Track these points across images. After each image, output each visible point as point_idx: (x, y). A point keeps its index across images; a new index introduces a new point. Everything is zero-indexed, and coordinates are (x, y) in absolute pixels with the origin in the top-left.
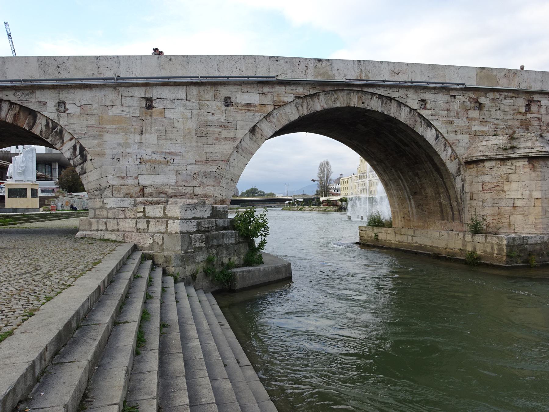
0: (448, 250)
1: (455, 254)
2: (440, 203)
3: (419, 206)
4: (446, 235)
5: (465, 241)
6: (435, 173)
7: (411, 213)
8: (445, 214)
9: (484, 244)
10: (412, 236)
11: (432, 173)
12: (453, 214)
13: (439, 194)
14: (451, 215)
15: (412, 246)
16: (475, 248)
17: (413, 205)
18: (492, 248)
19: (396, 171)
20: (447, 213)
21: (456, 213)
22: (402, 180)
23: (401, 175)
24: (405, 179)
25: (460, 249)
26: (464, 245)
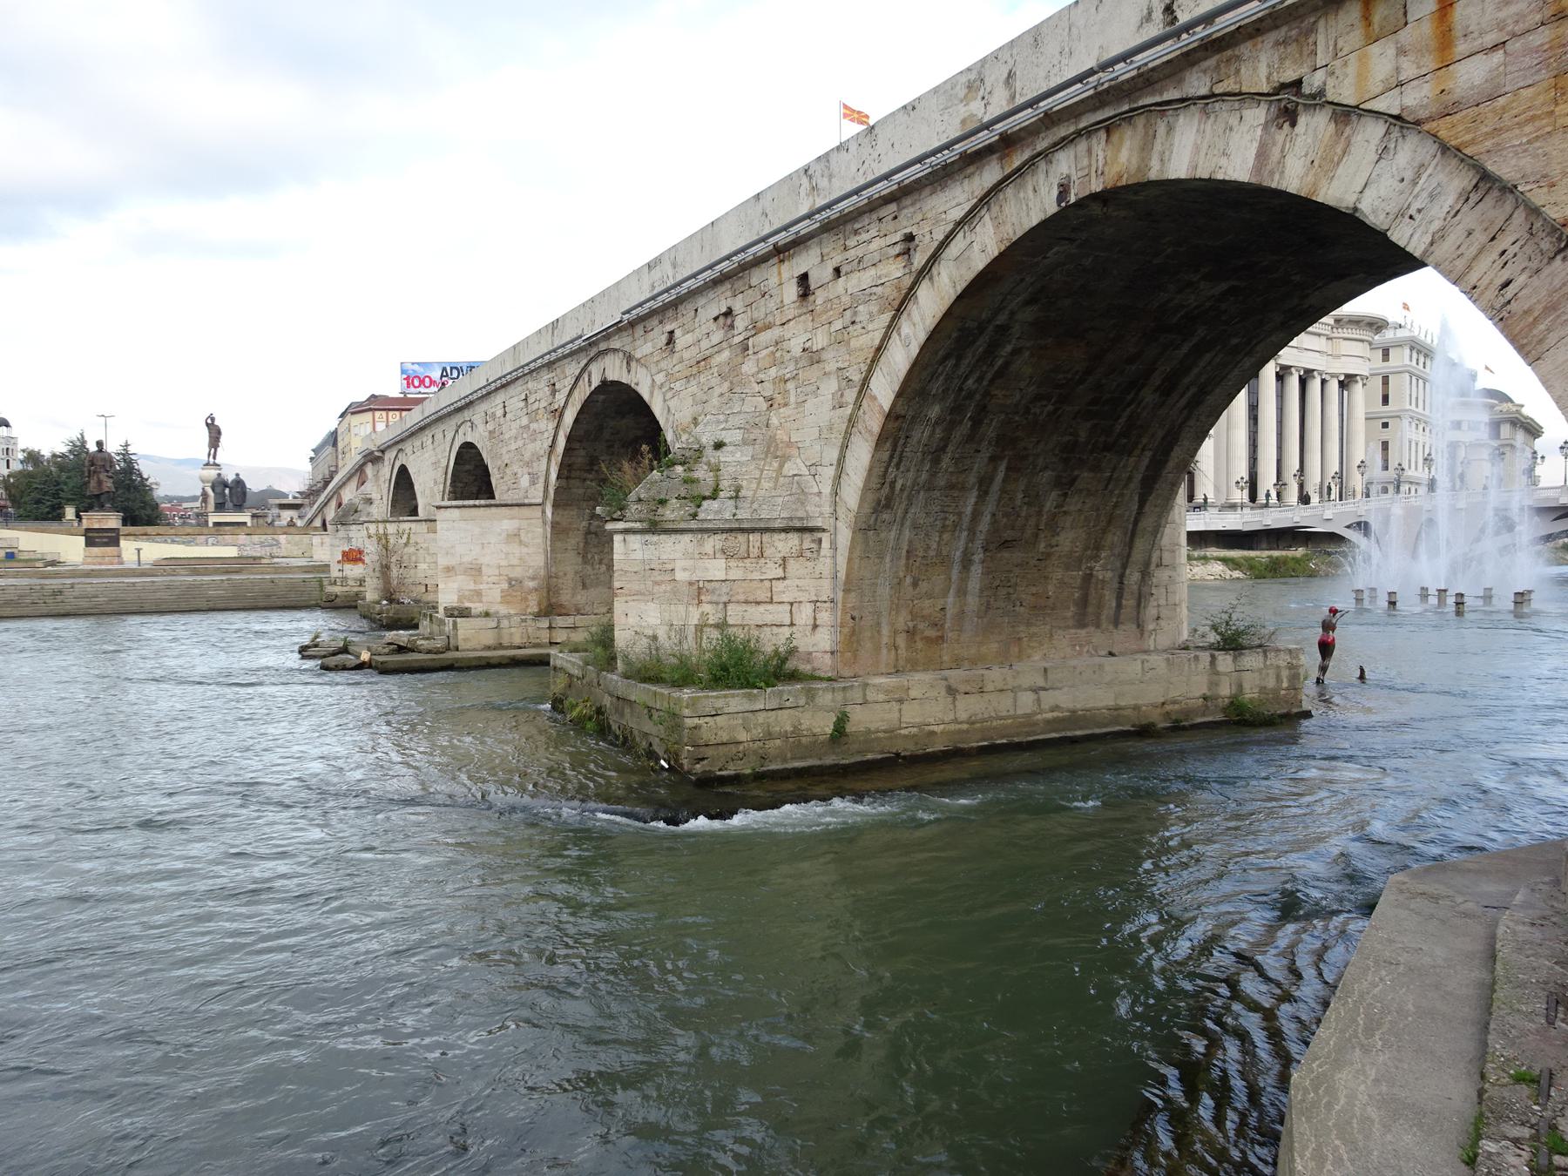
0: (1168, 708)
1: (1188, 713)
2: (1088, 577)
3: (998, 589)
4: (1163, 665)
5: (1218, 673)
6: (1135, 485)
7: (950, 612)
8: (1090, 610)
9: (1260, 671)
10: (1036, 690)
11: (1126, 486)
12: (1119, 606)
13: (1098, 547)
14: (1112, 612)
15: (1035, 724)
16: (1240, 686)
17: (975, 581)
18: (1278, 678)
19: (994, 459)
20: (1100, 606)
21: (1128, 602)
22: (983, 495)
23: (1000, 476)
24: (1003, 491)
25: (1205, 698)
26: (1213, 684)
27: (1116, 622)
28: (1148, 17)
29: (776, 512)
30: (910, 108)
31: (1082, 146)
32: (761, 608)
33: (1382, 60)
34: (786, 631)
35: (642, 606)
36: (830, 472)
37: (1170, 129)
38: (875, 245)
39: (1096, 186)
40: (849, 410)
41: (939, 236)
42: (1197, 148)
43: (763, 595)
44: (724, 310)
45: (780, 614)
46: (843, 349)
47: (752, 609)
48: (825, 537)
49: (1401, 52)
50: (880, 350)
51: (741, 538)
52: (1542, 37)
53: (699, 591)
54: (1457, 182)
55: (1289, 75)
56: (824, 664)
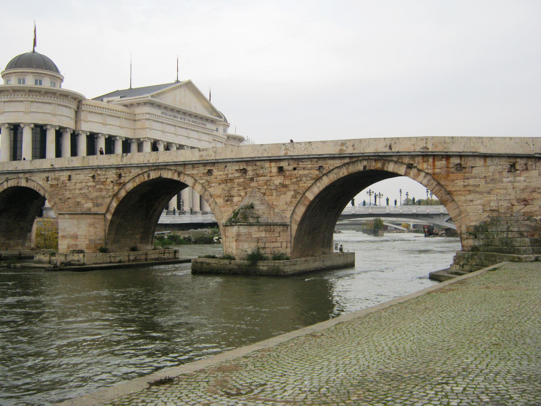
27: (327, 246)
28: (386, 146)
29: (277, 220)
30: (324, 142)
31: (370, 161)
32: (274, 243)
33: (425, 166)
34: (280, 249)
35: (243, 243)
36: (291, 212)
37: (388, 163)
38: (309, 166)
39: (372, 168)
40: (298, 199)
41: (331, 168)
42: (394, 168)
43: (274, 240)
44: (242, 168)
45: (279, 244)
46: (296, 186)
47: (272, 244)
48: (289, 227)
49: (428, 165)
50: (309, 188)
51: (269, 227)
52: (446, 169)
53: (258, 240)
54: (435, 183)
55: (411, 162)
56: (289, 255)
